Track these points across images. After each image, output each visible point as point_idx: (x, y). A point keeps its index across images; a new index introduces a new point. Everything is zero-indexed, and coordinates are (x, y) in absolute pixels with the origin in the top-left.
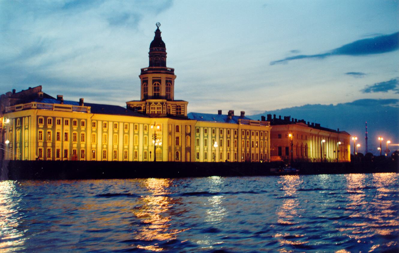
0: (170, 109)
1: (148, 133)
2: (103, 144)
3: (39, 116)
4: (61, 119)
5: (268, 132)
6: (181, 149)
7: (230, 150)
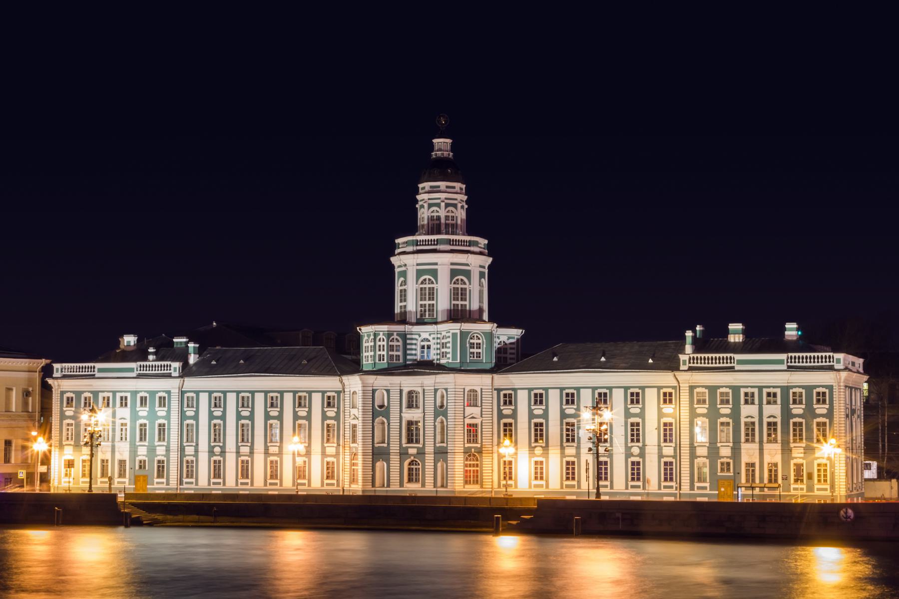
0: (429, 347)
1: (338, 413)
2: (212, 444)
4: (110, 395)
5: (830, 388)
7: (642, 454)
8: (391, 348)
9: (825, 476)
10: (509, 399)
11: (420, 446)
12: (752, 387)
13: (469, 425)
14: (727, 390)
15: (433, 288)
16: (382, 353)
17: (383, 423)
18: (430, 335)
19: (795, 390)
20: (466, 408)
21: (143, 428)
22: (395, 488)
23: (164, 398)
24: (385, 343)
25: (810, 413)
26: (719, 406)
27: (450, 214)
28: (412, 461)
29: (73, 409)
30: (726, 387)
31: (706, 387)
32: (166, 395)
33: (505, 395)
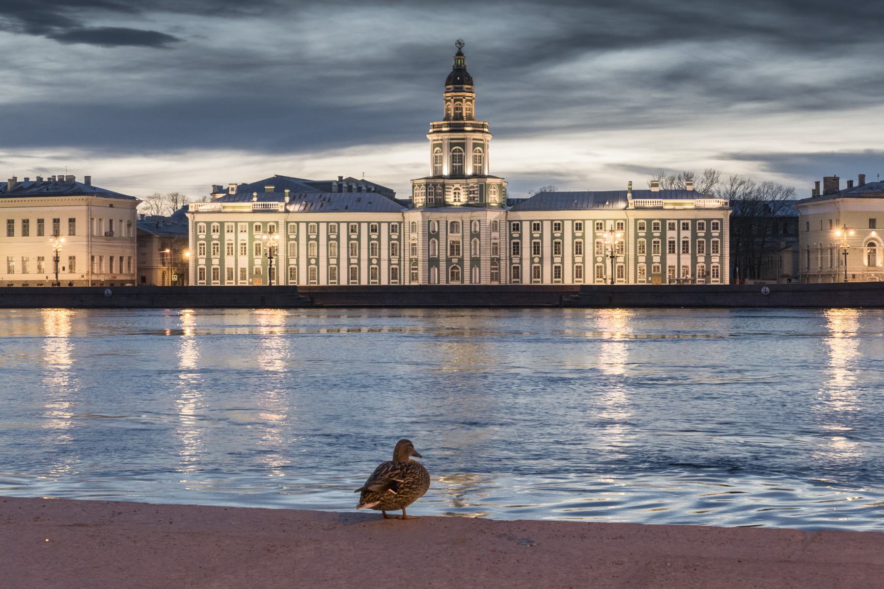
1: (400, 236)
2: (310, 257)
3: (199, 222)
4: (233, 224)
5: (721, 220)
6: (461, 261)
8: (436, 194)
9: (717, 273)
10: (517, 227)
11: (460, 257)
12: (674, 219)
13: (494, 244)
14: (658, 221)
15: (462, 155)
16: (431, 197)
17: (434, 242)
18: (461, 185)
19: (700, 221)
20: (492, 233)
21: (244, 246)
22: (443, 283)
23: (274, 226)
24: (433, 191)
25: (708, 236)
26: (653, 231)
27: (468, 107)
28: (454, 267)
29: (261, 234)
30: (658, 219)
31: (645, 220)
32: (275, 225)
33: (514, 225)
